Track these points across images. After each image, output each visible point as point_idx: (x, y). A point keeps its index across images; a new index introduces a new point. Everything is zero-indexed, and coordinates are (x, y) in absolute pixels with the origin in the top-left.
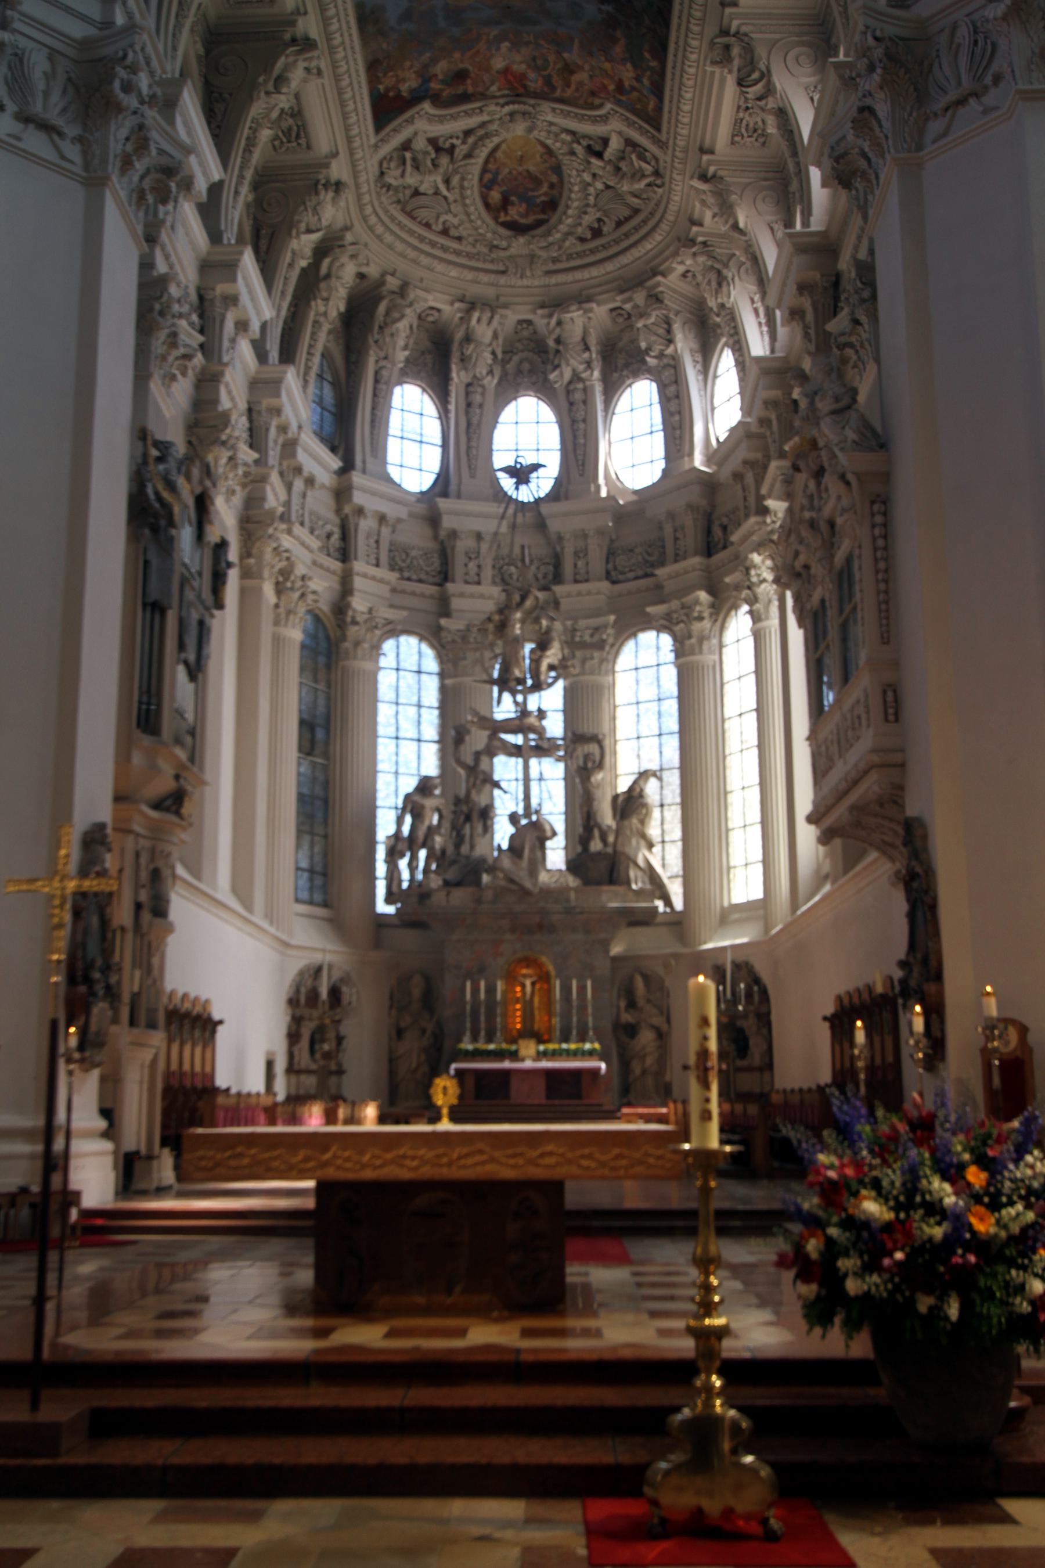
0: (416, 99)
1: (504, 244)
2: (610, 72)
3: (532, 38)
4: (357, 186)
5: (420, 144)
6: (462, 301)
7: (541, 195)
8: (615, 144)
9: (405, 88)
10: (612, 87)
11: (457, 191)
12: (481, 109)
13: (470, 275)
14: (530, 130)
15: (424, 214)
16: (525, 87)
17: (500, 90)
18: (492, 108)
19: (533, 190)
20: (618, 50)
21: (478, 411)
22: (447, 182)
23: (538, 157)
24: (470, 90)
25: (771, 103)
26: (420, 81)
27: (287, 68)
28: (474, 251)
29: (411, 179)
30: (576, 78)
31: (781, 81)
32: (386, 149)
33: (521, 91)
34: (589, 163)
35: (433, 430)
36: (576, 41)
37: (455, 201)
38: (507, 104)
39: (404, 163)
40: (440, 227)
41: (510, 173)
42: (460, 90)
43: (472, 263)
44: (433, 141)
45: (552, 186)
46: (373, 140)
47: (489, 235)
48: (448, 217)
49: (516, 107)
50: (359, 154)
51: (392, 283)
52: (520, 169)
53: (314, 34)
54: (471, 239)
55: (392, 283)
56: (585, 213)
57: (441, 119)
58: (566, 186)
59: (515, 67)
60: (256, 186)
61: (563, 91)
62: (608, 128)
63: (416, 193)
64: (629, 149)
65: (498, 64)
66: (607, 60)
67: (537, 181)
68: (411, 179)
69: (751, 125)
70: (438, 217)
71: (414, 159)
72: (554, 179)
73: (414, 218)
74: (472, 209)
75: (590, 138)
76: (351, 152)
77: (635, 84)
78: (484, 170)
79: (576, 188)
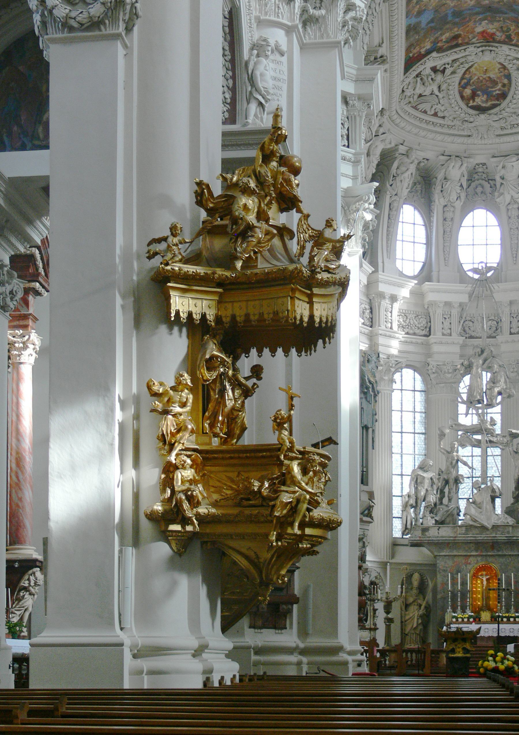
1: (472, 119)
6: (443, 155)
7: (497, 90)
13: (450, 139)
19: (492, 88)
21: (450, 223)
23: (497, 70)
28: (453, 124)
35: (421, 233)
37: (443, 97)
40: (433, 112)
41: (478, 78)
43: (452, 132)
45: (504, 85)
47: (463, 115)
51: (402, 149)
52: (485, 76)
54: (451, 118)
55: (402, 149)
67: (495, 83)
72: (506, 81)
73: (418, 110)
78: (462, 78)
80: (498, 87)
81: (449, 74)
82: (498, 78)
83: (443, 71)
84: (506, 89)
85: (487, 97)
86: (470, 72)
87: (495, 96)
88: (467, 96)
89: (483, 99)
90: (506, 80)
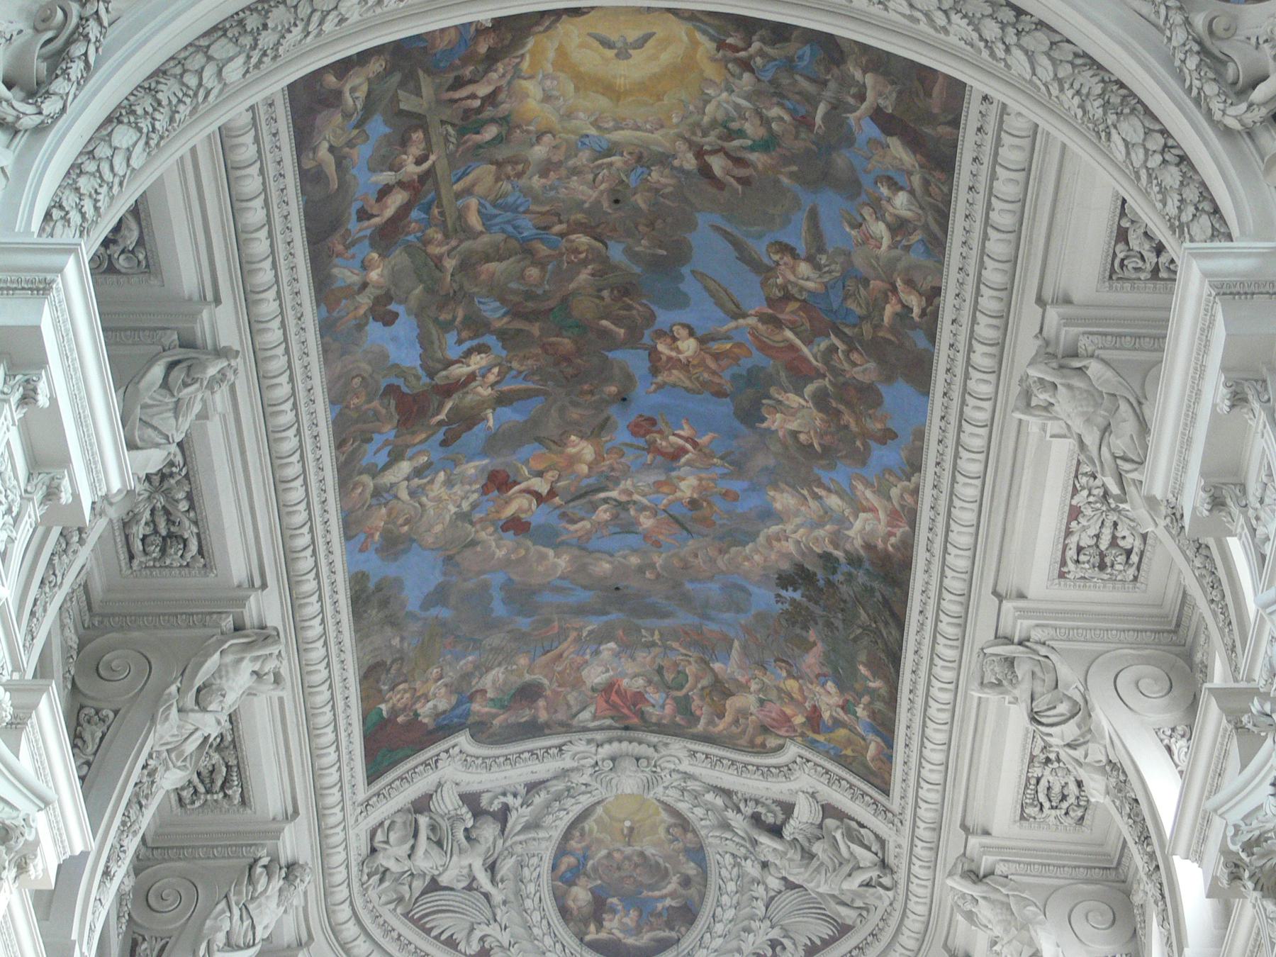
0: (444, 728)
2: (796, 696)
3: (657, 637)
4: (326, 872)
5: (448, 802)
7: (667, 895)
8: (805, 813)
9: (425, 711)
10: (799, 720)
11: (509, 884)
12: (560, 748)
14: (648, 786)
15: (443, 923)
16: (641, 714)
17: (595, 718)
18: (581, 747)
19: (651, 888)
20: (811, 660)
22: (492, 868)
23: (661, 832)
24: (543, 716)
25: (1096, 753)
26: (454, 699)
27: (219, 672)
29: (428, 860)
30: (733, 704)
31: (1107, 715)
32: (383, 810)
33: (635, 721)
34: (755, 843)
36: (736, 644)
37: (505, 903)
38: (610, 741)
39: (415, 836)
41: (609, 855)
42: (525, 715)
44: (471, 800)
45: (686, 882)
46: (362, 795)
48: (493, 930)
49: (625, 745)
50: (335, 817)
52: (628, 850)
53: (274, 618)
56: (748, 930)
57: (487, 764)
58: (713, 881)
59: (625, 682)
60: (138, 867)
61: (711, 722)
62: (794, 786)
63: (434, 886)
64: (831, 823)
65: (595, 675)
66: (790, 675)
68: (428, 860)
69: (1056, 789)
70: (472, 929)
71: (433, 828)
72: (691, 869)
74: (536, 916)
75: (757, 802)
76: (320, 814)
77: (842, 715)
78: (561, 851)
79: (731, 887)
80: (670, 888)
81: (519, 827)
82: (667, 858)
83: (502, 816)
84: (693, 892)
85: (640, 915)
86: (582, 835)
87: (660, 915)
88: (579, 908)
89: (626, 920)
90: (692, 864)
